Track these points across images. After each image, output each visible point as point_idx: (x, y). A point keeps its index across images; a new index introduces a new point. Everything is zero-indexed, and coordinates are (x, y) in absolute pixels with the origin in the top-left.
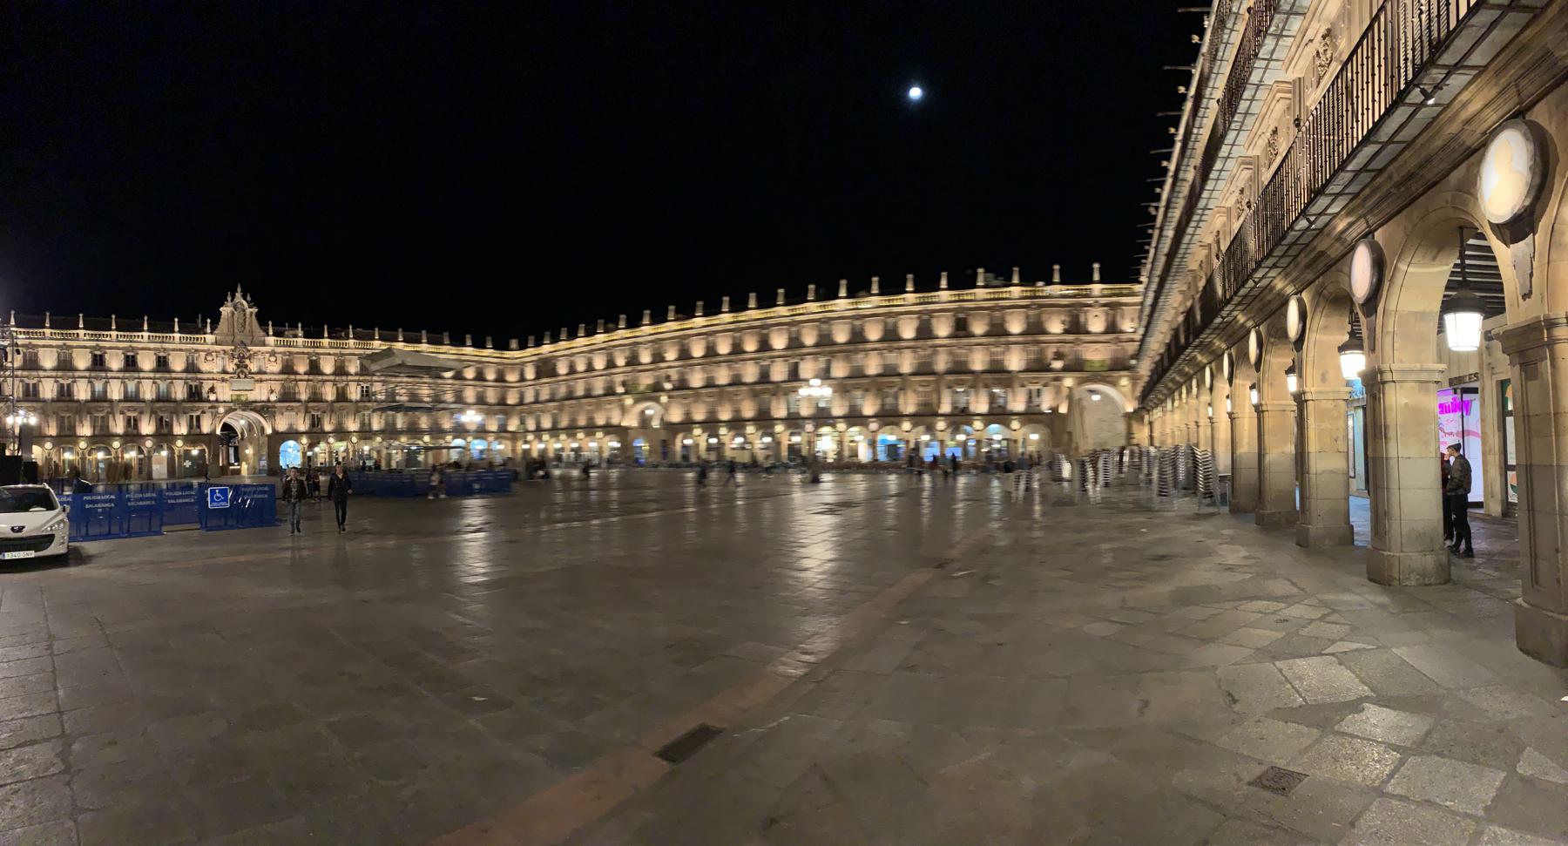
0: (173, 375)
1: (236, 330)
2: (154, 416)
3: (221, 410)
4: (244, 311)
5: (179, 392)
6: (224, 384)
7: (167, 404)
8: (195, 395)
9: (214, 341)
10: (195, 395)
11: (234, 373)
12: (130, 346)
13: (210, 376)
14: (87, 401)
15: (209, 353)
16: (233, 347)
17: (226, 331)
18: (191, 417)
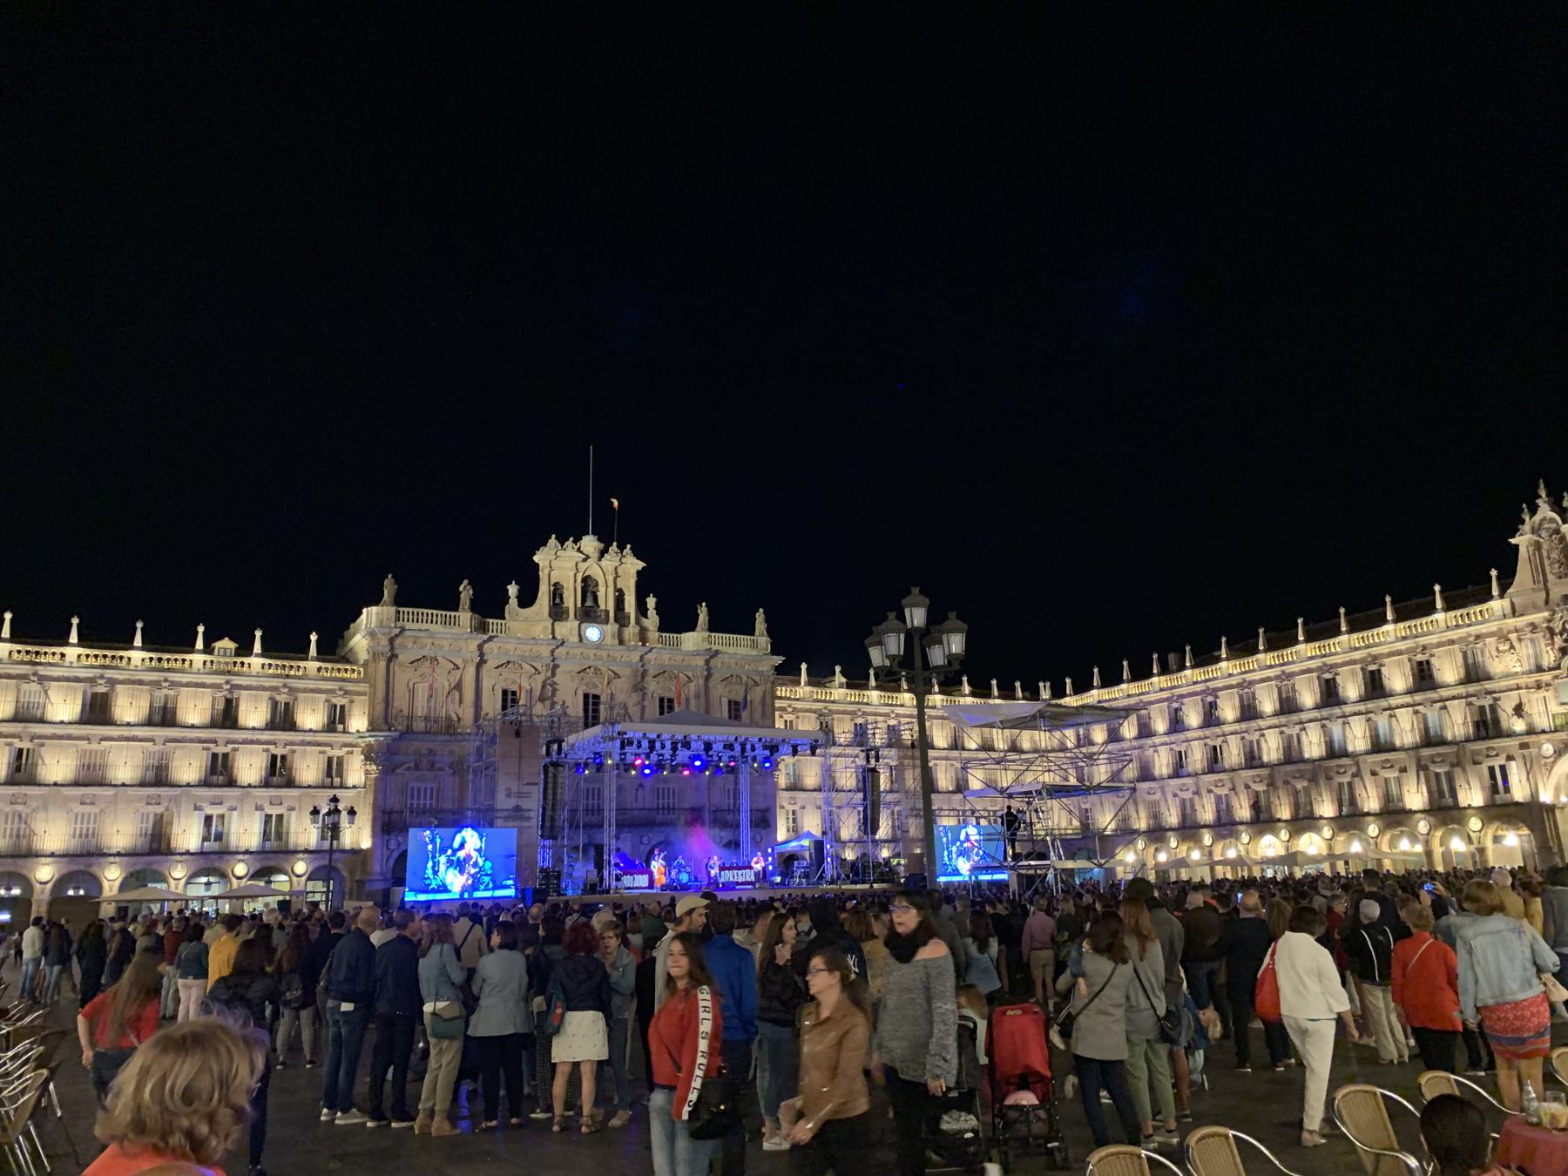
0: (1444, 693)
1: (1550, 577)
2: (1422, 773)
3: (1548, 749)
4: (1557, 531)
5: (1457, 723)
6: (1542, 693)
7: (1440, 750)
8: (1487, 726)
9: (1508, 610)
10: (1487, 726)
11: (1558, 667)
12: (1369, 655)
13: (1512, 682)
14: (1321, 759)
15: (1502, 636)
16: (1546, 614)
17: (1529, 583)
18: (1491, 769)
